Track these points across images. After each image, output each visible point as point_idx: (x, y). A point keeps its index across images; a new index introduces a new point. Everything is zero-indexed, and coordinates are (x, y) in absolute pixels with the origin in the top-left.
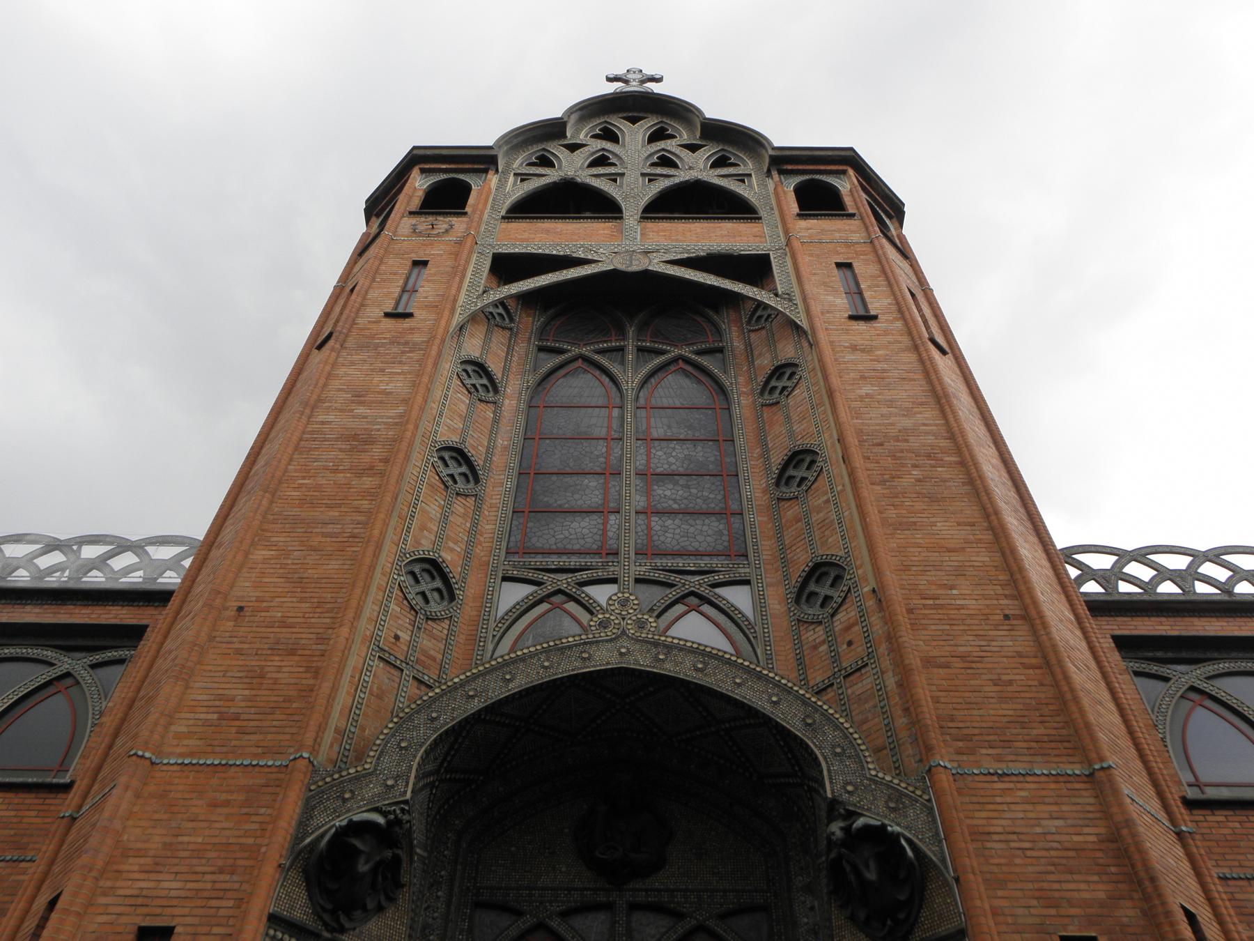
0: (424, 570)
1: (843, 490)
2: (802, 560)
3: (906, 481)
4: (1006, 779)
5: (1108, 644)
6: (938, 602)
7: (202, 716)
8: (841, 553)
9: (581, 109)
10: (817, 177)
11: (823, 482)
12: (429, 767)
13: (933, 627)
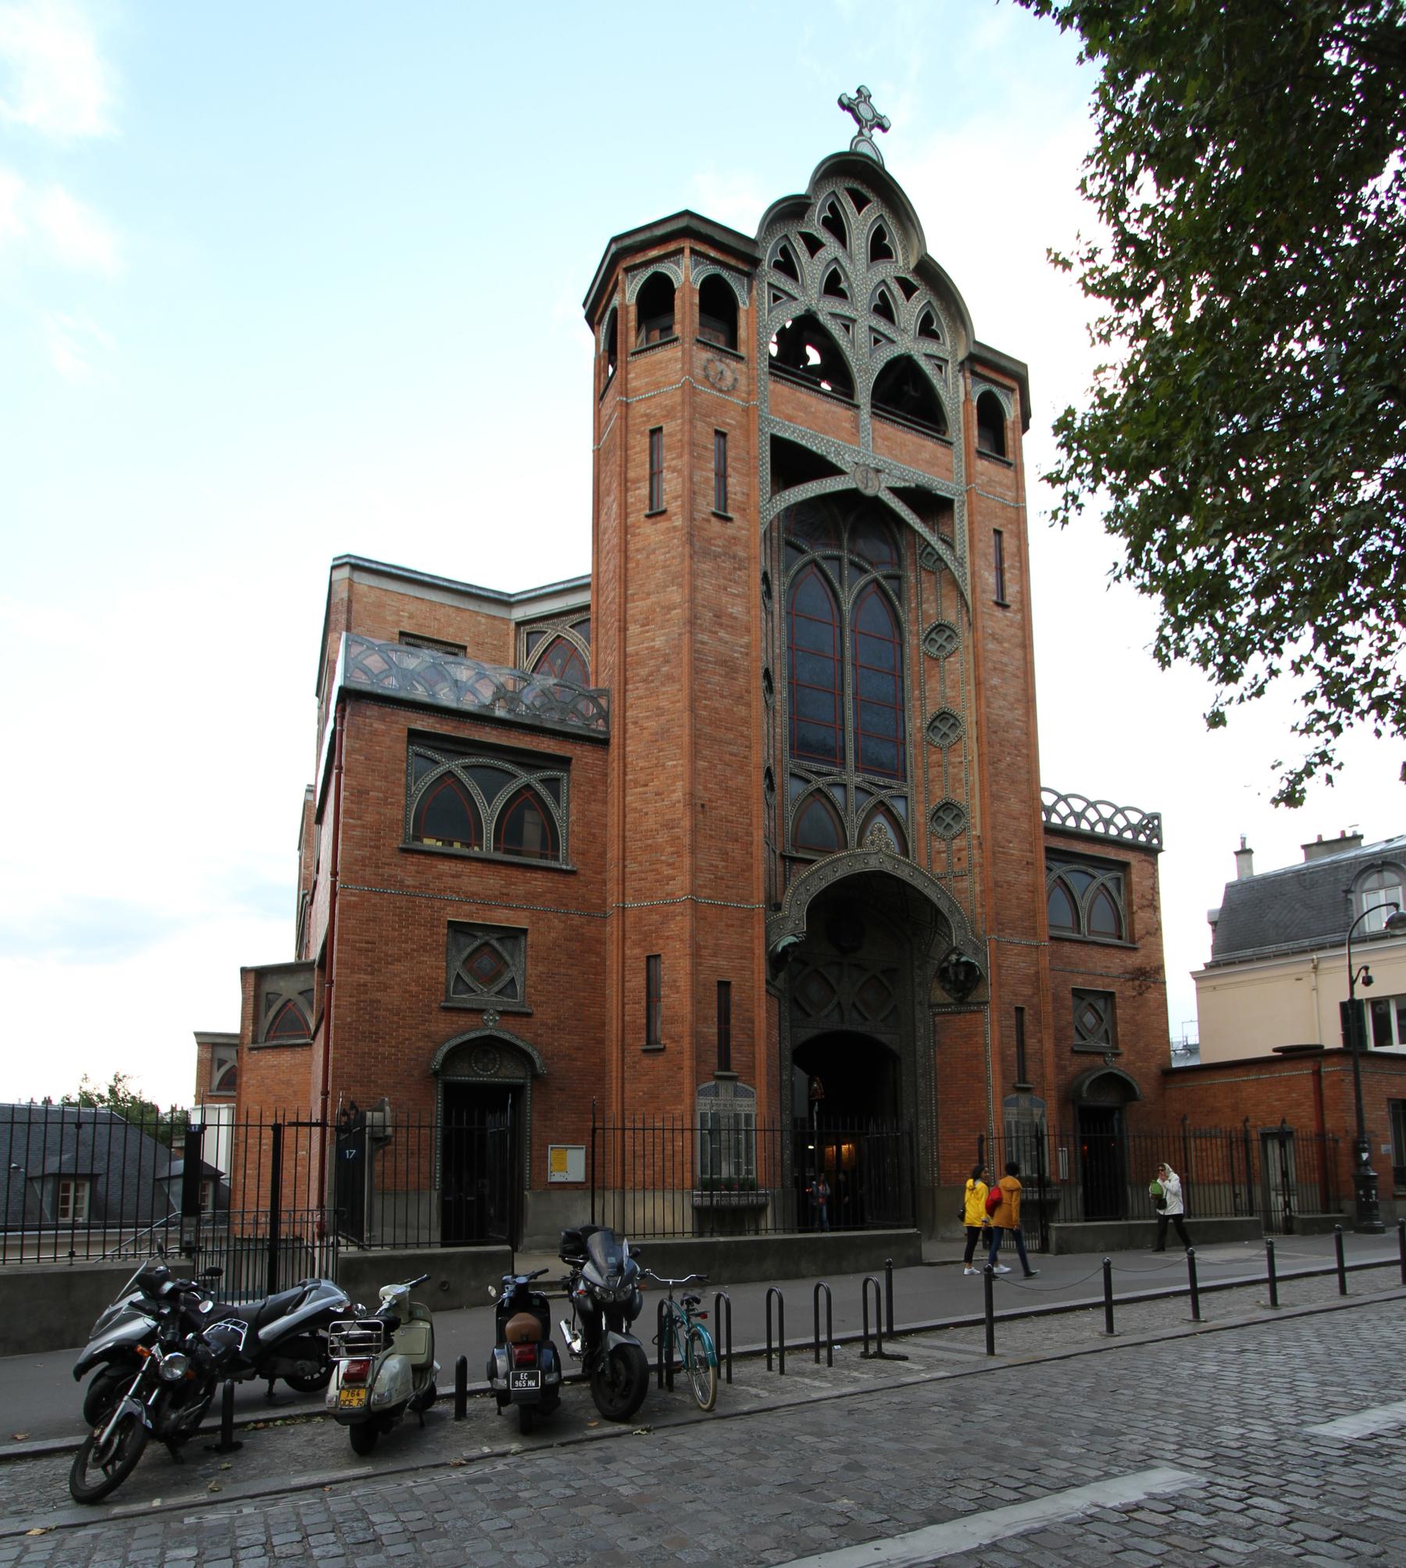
2: (939, 795)
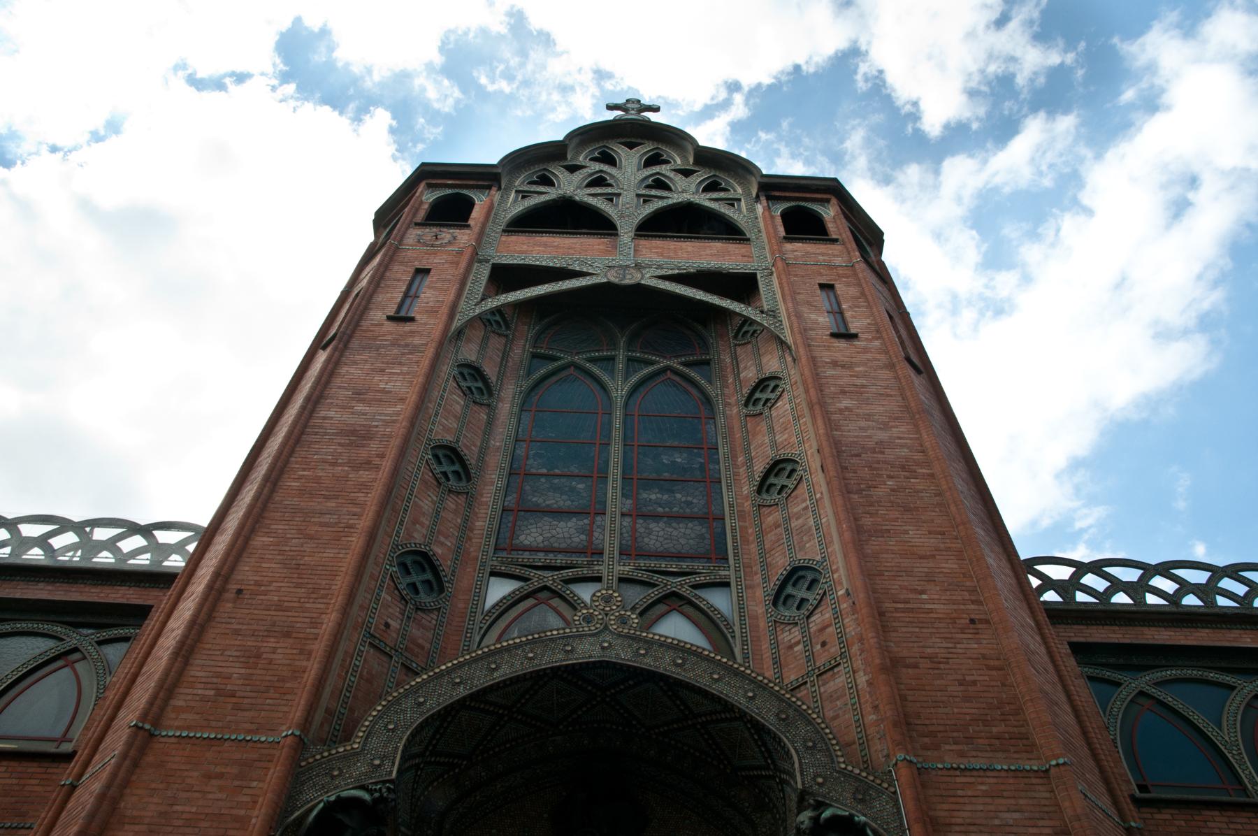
0: (415, 562)
1: (821, 498)
2: (781, 563)
3: (881, 491)
4: (968, 773)
5: (1066, 649)
6: (908, 606)
7: (200, 692)
8: (818, 558)
9: (581, 134)
10: (803, 204)
11: (803, 487)
12: (416, 750)
13: (904, 630)
